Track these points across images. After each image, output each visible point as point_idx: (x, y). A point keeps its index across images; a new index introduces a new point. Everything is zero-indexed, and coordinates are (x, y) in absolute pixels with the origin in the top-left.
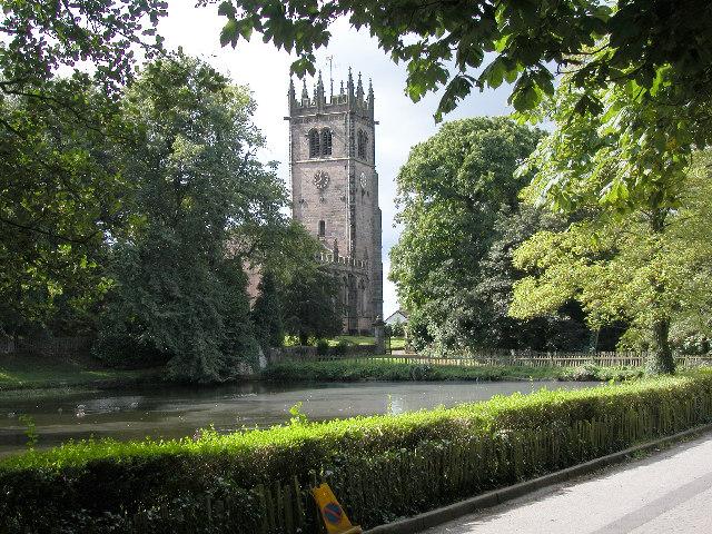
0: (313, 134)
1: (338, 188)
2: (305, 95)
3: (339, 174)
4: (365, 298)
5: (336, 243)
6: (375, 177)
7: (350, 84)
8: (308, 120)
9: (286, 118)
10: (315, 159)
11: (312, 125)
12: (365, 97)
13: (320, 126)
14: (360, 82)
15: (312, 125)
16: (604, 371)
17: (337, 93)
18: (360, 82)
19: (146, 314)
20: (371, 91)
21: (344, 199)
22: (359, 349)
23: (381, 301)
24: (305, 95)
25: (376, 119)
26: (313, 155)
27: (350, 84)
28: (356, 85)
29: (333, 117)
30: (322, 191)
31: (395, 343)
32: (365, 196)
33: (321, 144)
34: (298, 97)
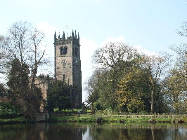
0: (61, 49)
1: (69, 64)
2: (59, 37)
3: (69, 59)
4: (77, 97)
5: (69, 80)
6: (80, 61)
7: (73, 33)
8: (60, 44)
9: (53, 43)
10: (62, 55)
11: (61, 46)
12: (77, 38)
13: (64, 46)
14: (76, 34)
15: (61, 46)
16: (157, 119)
17: (69, 36)
18: (76, 34)
19: (79, 111)
20: (79, 35)
21: (70, 68)
22: (66, 113)
23: (81, 98)
24: (59, 37)
25: (80, 44)
26: (61, 54)
27: (73, 33)
28: (74, 34)
29: (68, 43)
30: (64, 65)
31: (88, 111)
32: (77, 67)
33: (64, 51)
34: (57, 38)
